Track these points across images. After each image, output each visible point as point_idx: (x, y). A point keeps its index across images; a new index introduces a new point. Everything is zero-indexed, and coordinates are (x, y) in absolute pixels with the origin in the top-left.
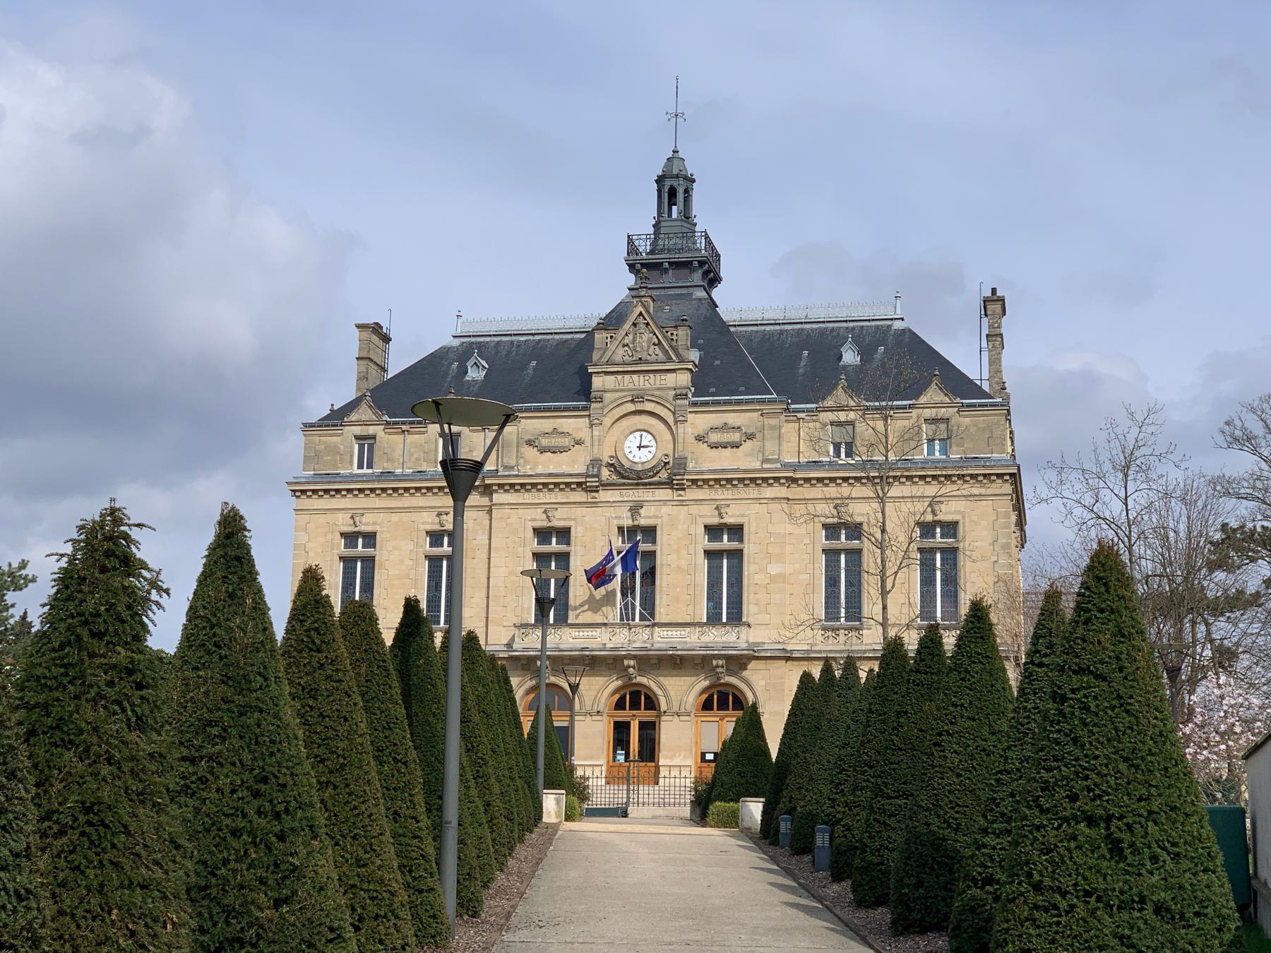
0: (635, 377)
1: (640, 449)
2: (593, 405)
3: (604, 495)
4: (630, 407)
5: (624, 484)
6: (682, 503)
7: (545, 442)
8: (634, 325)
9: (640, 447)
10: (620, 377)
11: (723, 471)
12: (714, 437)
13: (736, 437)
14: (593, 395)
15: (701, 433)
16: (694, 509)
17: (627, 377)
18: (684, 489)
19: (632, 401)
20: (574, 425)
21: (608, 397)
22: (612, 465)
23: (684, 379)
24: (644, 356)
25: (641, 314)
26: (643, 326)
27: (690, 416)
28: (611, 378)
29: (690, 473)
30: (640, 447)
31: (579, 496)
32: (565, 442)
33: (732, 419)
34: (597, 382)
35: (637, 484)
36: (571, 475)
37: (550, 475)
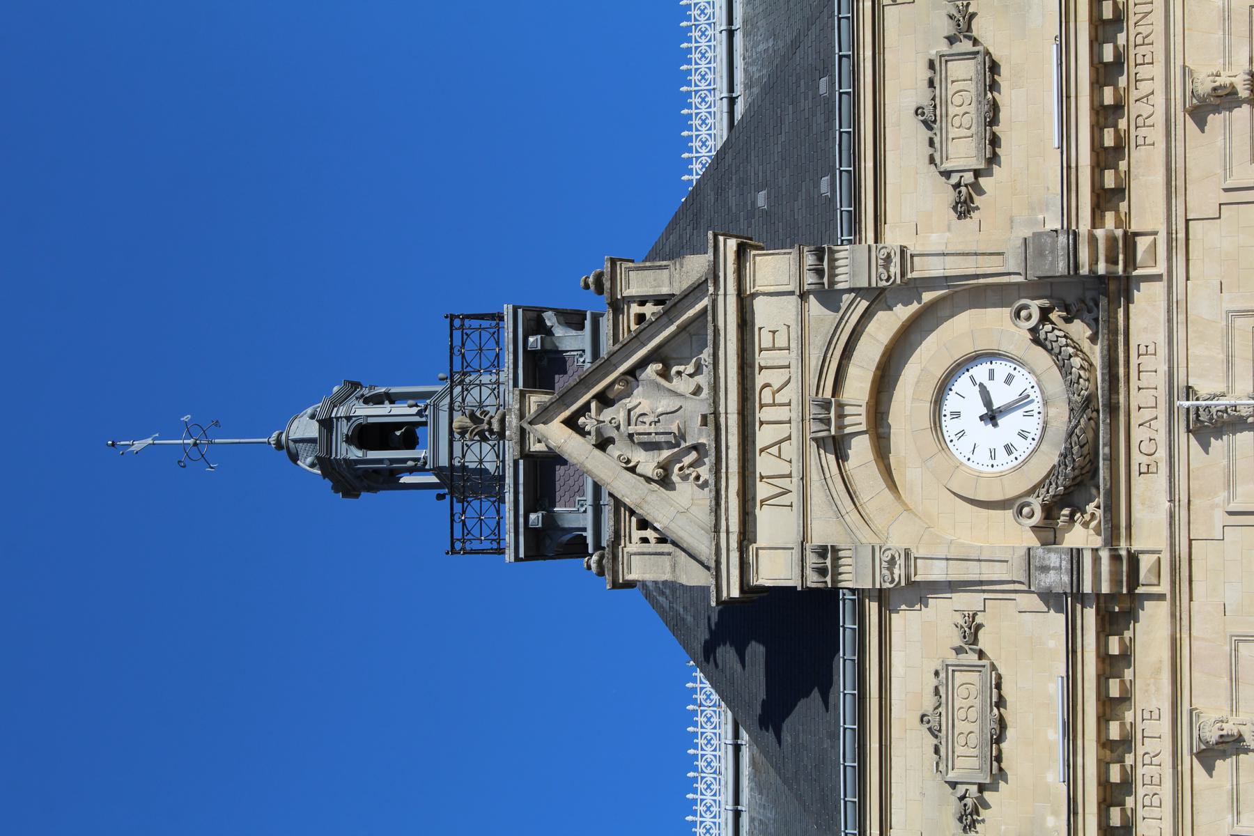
0: (764, 436)
1: (991, 417)
2: (849, 580)
3: (1149, 533)
4: (860, 449)
5: (1113, 459)
6: (1179, 241)
7: (968, 763)
8: (603, 444)
9: (992, 417)
10: (762, 490)
11: (1065, 97)
12: (963, 152)
13: (963, 72)
14: (813, 580)
15: (951, 196)
16: (1202, 196)
17: (764, 464)
18: (1130, 240)
19: (838, 446)
20: (915, 647)
21: (818, 537)
22: (1050, 511)
23: (773, 270)
24: (701, 406)
25: (571, 423)
26: (607, 414)
27: (893, 238)
28: (764, 517)
29: (1068, 212)
30: (992, 417)
31: (1151, 631)
32: (968, 690)
33: (904, 89)
34: (776, 569)
35: (1113, 409)
36: (1072, 652)
37: (1070, 730)
